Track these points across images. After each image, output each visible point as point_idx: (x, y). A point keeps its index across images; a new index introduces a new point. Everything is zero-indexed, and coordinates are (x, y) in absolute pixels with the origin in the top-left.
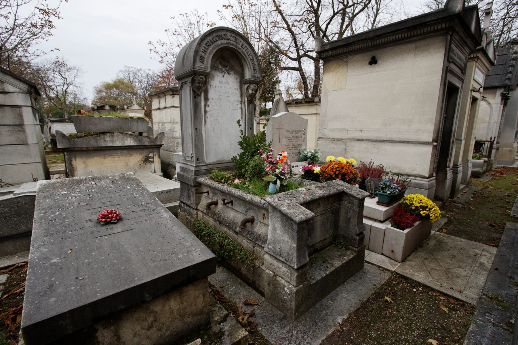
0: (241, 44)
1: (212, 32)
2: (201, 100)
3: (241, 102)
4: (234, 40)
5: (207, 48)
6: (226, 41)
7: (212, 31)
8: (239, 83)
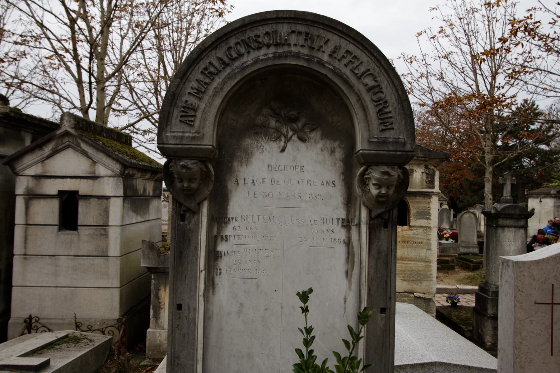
0: (329, 49)
3: (347, 224)
4: (301, 41)
5: (207, 80)
6: (272, 50)
8: (340, 165)
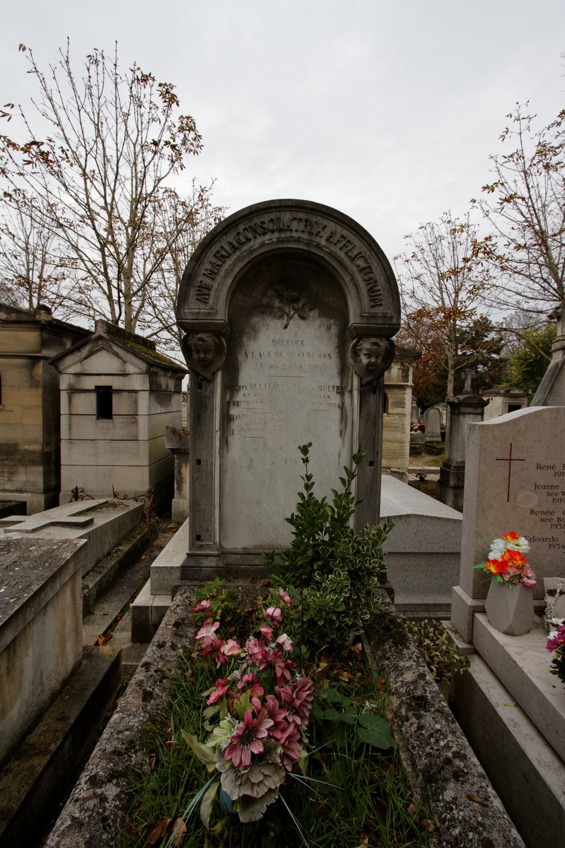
0: (326, 234)
1: (235, 222)
2: (213, 392)
3: (341, 391)
4: (301, 226)
5: (219, 263)
6: (276, 235)
7: (235, 218)
8: (335, 340)
